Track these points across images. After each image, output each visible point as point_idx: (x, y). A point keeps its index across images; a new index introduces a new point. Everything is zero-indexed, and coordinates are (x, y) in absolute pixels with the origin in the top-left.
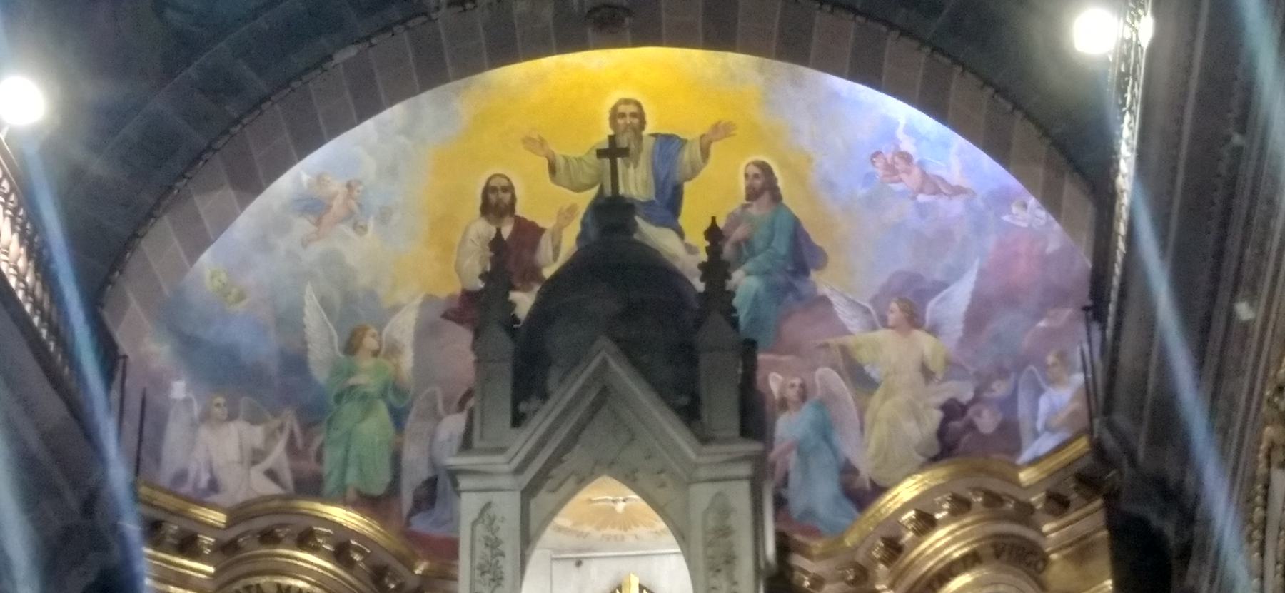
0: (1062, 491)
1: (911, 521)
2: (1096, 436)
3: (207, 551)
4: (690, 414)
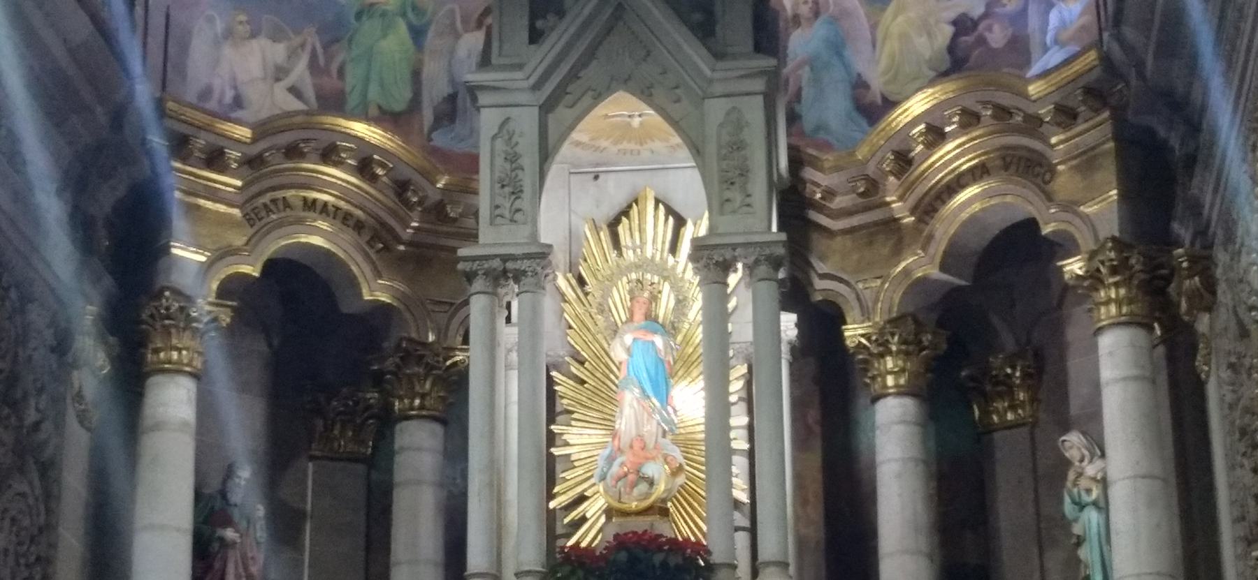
0: (1070, 104)
1: (921, 134)
2: (1105, 48)
3: (234, 166)
4: (705, 30)
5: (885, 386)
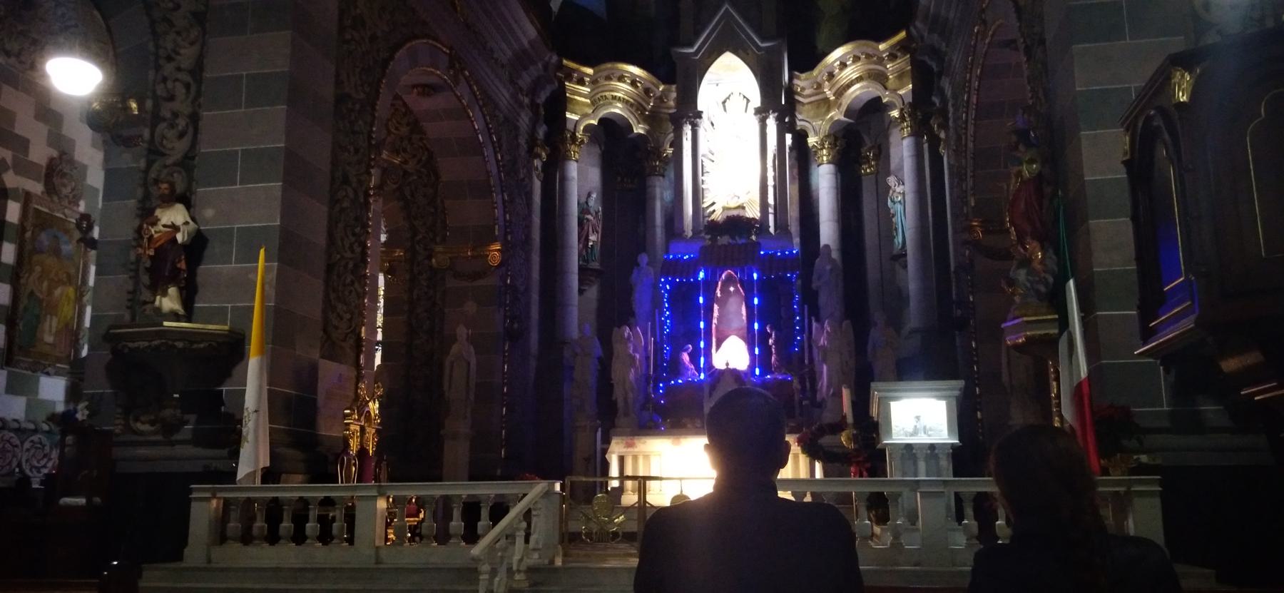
3: (587, 84)
5: (823, 160)
